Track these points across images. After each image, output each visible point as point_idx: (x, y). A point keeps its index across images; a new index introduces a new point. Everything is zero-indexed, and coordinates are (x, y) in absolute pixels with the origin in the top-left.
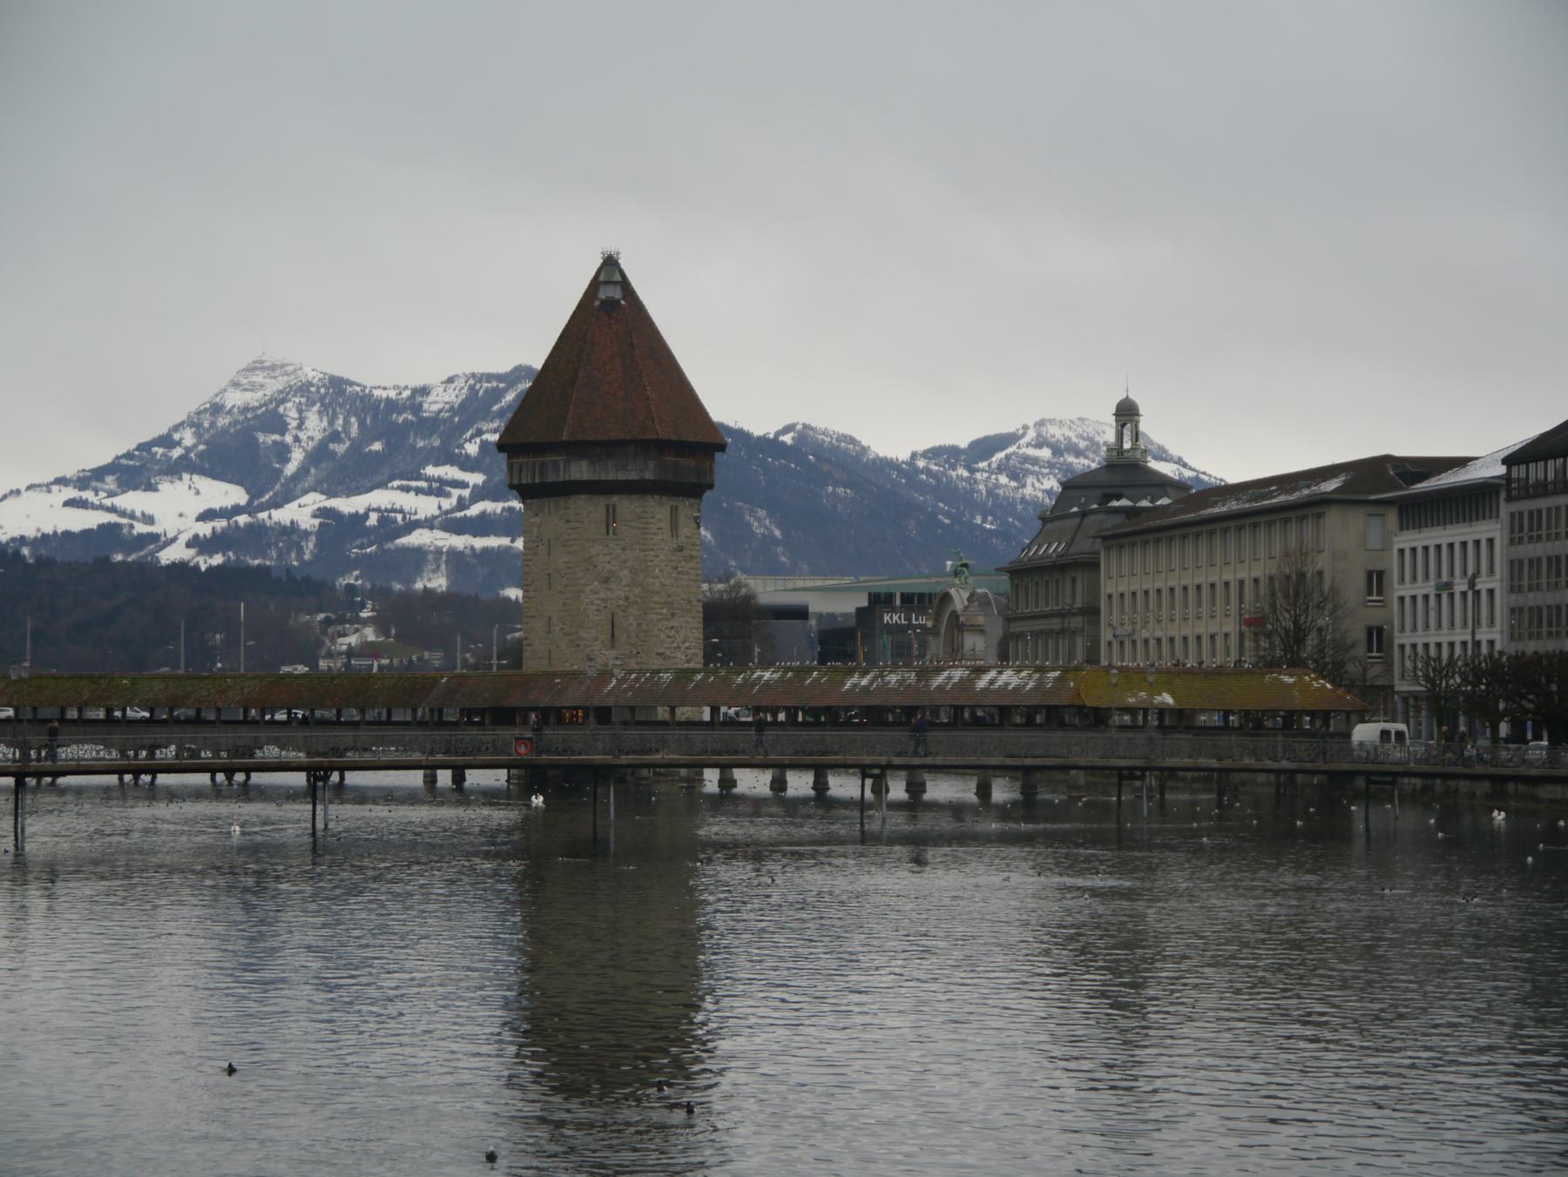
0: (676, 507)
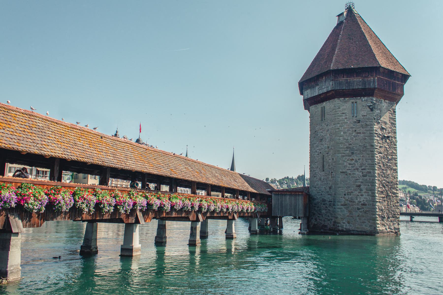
0: (356, 102)
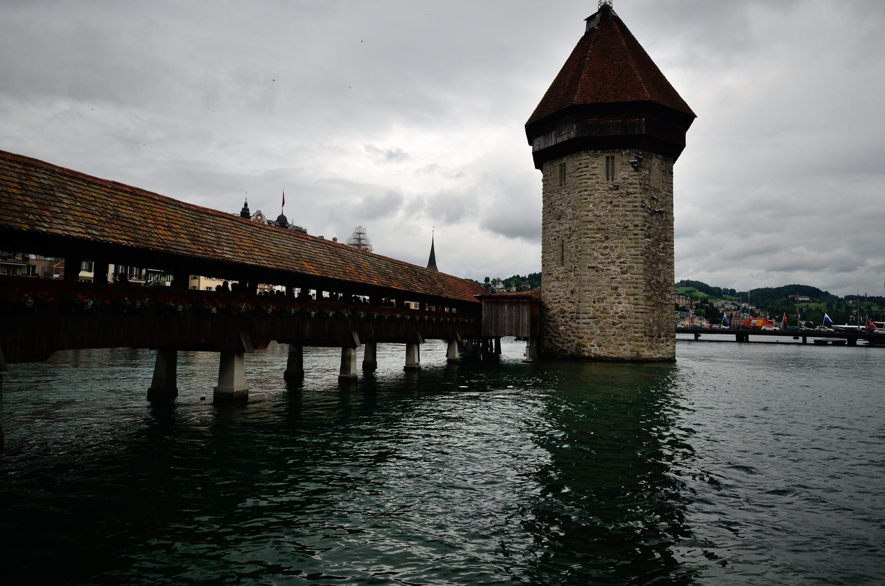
0: (613, 158)
